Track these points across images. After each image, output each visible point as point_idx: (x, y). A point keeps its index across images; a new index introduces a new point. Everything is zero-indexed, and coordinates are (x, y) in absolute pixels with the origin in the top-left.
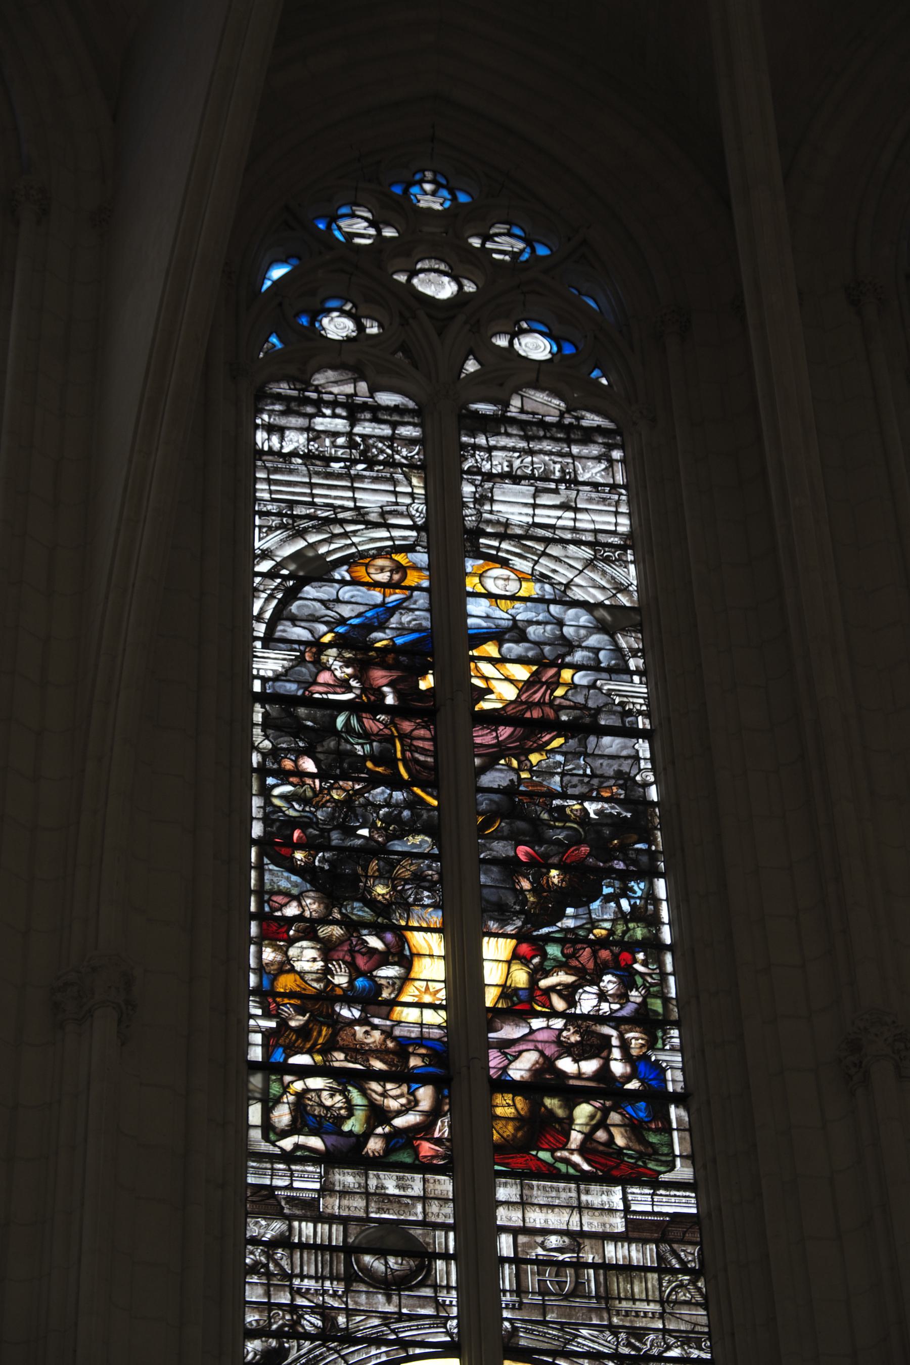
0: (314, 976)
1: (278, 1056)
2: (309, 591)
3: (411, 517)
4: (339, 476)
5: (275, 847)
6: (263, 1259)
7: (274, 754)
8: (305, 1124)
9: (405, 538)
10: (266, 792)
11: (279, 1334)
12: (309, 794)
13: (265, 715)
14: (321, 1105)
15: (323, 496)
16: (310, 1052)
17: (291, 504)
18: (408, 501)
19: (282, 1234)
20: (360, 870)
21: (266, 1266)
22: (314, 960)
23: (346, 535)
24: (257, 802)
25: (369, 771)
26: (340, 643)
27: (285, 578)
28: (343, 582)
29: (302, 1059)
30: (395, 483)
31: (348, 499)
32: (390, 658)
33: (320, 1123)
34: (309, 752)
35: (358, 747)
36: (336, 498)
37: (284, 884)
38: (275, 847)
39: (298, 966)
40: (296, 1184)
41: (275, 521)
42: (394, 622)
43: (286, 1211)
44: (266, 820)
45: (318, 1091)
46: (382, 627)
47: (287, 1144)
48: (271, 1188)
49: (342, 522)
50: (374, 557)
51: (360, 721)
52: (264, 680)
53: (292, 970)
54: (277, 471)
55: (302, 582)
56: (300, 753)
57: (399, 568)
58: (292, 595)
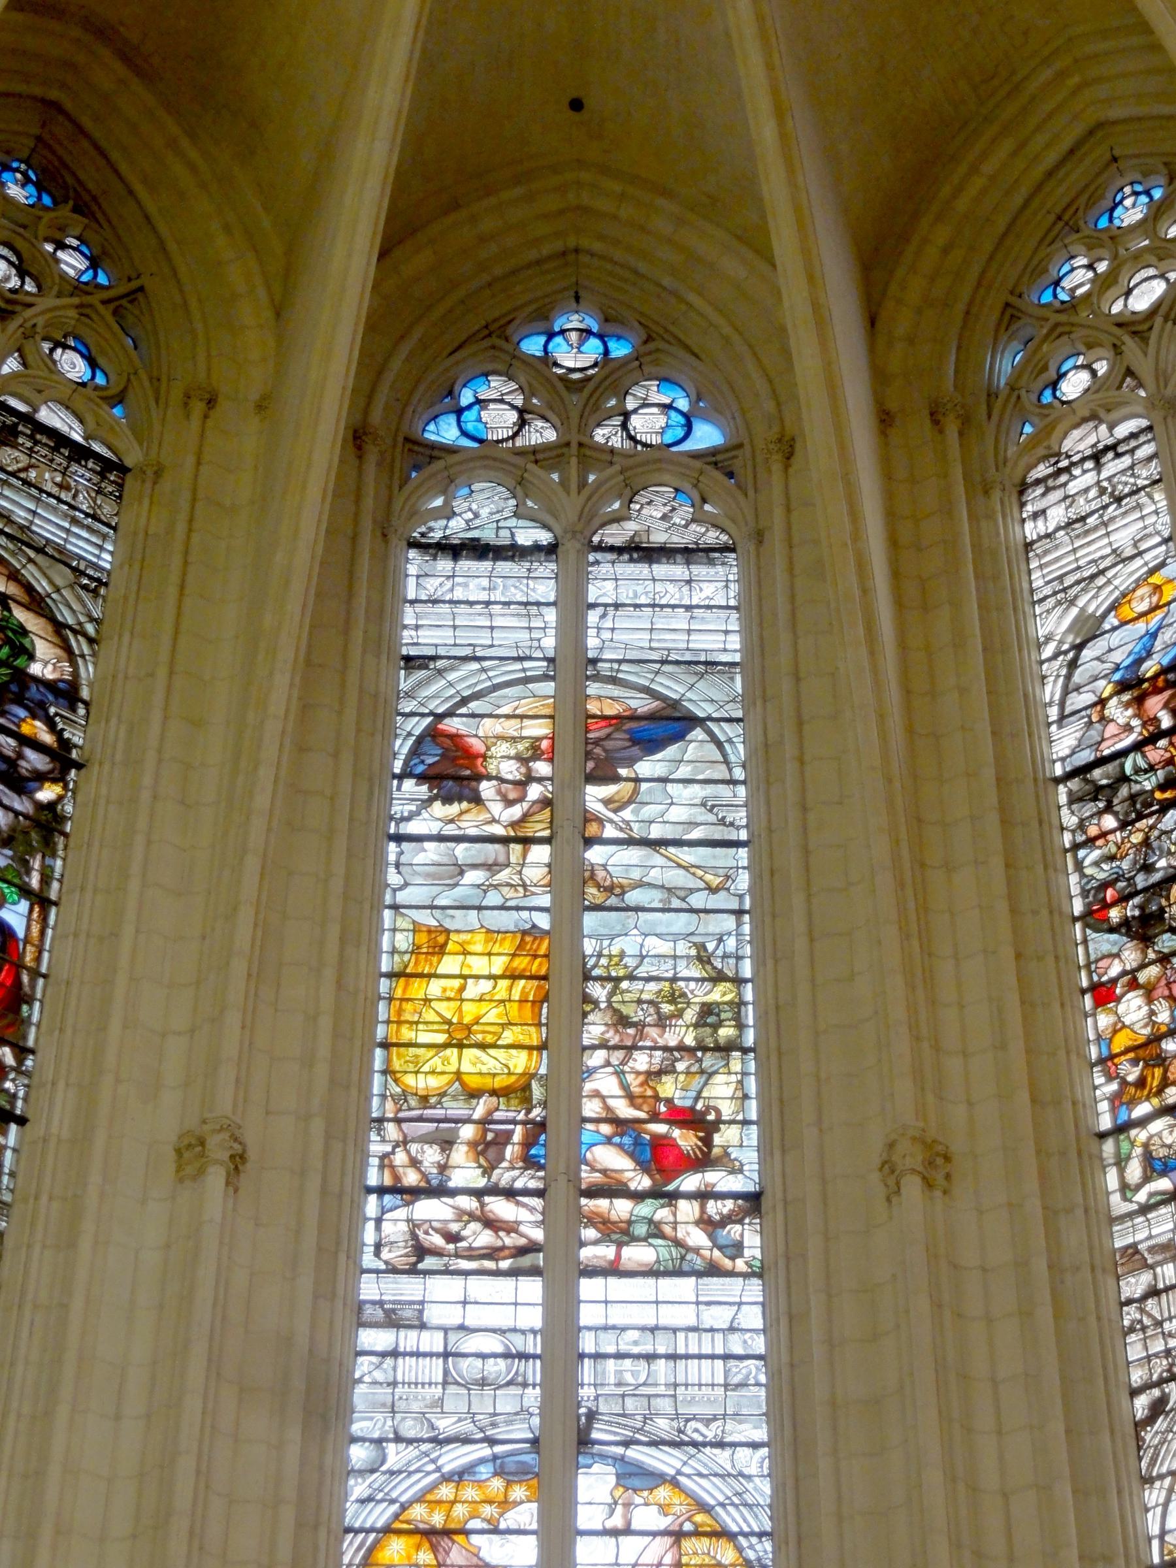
0: (1142, 1023)
1: (1123, 1116)
2: (1087, 654)
3: (1158, 533)
4: (1095, 528)
5: (1094, 918)
6: (1138, 1316)
7: (1081, 826)
8: (1153, 1170)
9: (1156, 557)
10: (1079, 866)
11: (1161, 1382)
12: (1114, 850)
13: (1070, 793)
14: (1164, 1145)
15: (1086, 554)
16: (1148, 1098)
17: (1060, 578)
18: (1153, 519)
19: (1149, 1285)
20: (1164, 902)
21: (1140, 1322)
22: (1140, 1007)
23: (1109, 582)
24: (1074, 879)
25: (1160, 802)
26: (1123, 687)
27: (1066, 653)
28: (1114, 629)
29: (1143, 1109)
30: (1139, 507)
31: (1104, 547)
32: (1160, 682)
33: (1165, 1164)
34: (1109, 809)
35: (1146, 783)
36: (1095, 551)
37: (1106, 948)
38: (1094, 918)
39: (1127, 1022)
40: (1154, 1232)
41: (1051, 602)
42: (1158, 645)
43: (1150, 1261)
44: (1085, 893)
45: (1159, 1135)
46: (1149, 654)
47: (1141, 1197)
48: (1134, 1246)
49: (1102, 572)
50: (1134, 590)
51: (1144, 756)
52: (1063, 760)
53: (1124, 1026)
54: (1046, 552)
55: (1079, 648)
56: (1100, 813)
57: (1157, 588)
58: (1073, 665)
